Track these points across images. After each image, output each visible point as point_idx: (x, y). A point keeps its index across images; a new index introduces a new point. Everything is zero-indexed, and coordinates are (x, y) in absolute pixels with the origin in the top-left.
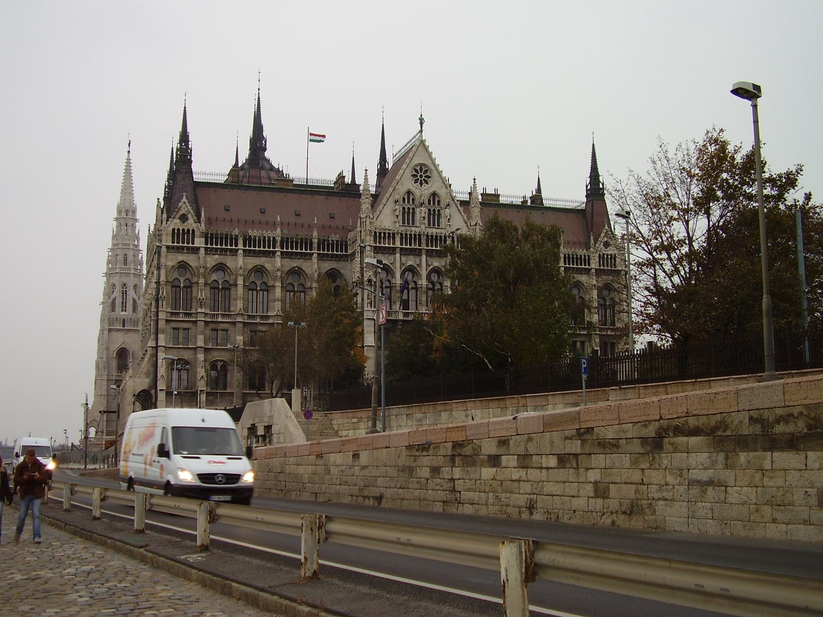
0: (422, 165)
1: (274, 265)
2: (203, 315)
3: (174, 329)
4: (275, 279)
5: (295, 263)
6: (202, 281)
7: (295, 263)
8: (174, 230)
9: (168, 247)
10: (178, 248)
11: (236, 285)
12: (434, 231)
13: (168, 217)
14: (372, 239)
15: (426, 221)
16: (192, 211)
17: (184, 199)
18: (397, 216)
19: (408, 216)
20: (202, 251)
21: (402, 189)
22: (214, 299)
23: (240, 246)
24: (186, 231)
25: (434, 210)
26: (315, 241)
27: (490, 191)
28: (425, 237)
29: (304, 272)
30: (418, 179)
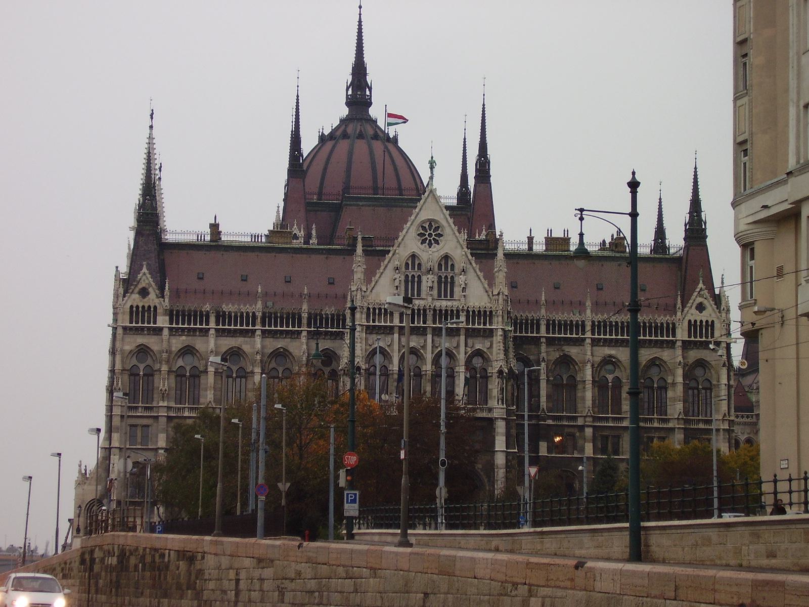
0: (430, 221)
1: (253, 347)
2: (165, 409)
3: (131, 426)
4: (253, 363)
5: (280, 343)
6: (165, 368)
7: (280, 343)
8: (132, 307)
9: (125, 328)
10: (137, 329)
11: (206, 372)
12: (444, 304)
13: (126, 292)
14: (364, 316)
15: (435, 292)
16: (153, 284)
17: (145, 270)
18: (397, 287)
19: (411, 285)
20: (166, 332)
22: (180, 388)
23: (212, 325)
24: (146, 309)
25: (446, 277)
26: (305, 315)
27: (558, 234)
28: (432, 312)
29: (290, 353)
30: (426, 238)
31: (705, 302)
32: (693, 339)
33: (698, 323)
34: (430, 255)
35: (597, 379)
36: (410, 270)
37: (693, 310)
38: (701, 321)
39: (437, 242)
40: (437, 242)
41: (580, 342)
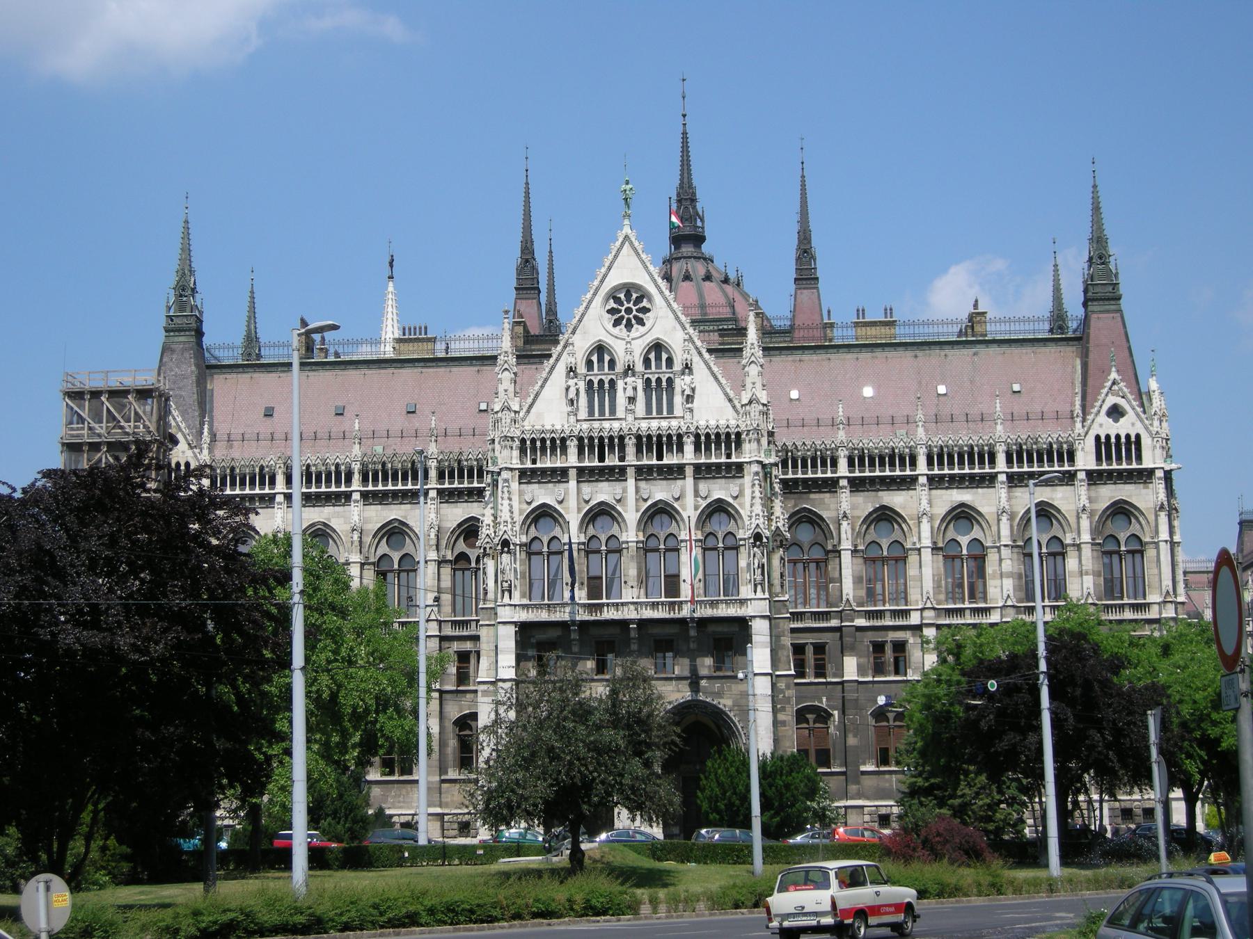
0: (629, 289)
12: (654, 426)
18: (572, 401)
21: (581, 344)
25: (659, 380)
26: (433, 464)
30: (622, 317)
31: (1122, 402)
32: (1104, 466)
33: (1113, 440)
34: (629, 346)
35: (940, 545)
36: (596, 371)
37: (1103, 418)
38: (1118, 437)
39: (641, 322)
40: (641, 322)
41: (908, 483)
